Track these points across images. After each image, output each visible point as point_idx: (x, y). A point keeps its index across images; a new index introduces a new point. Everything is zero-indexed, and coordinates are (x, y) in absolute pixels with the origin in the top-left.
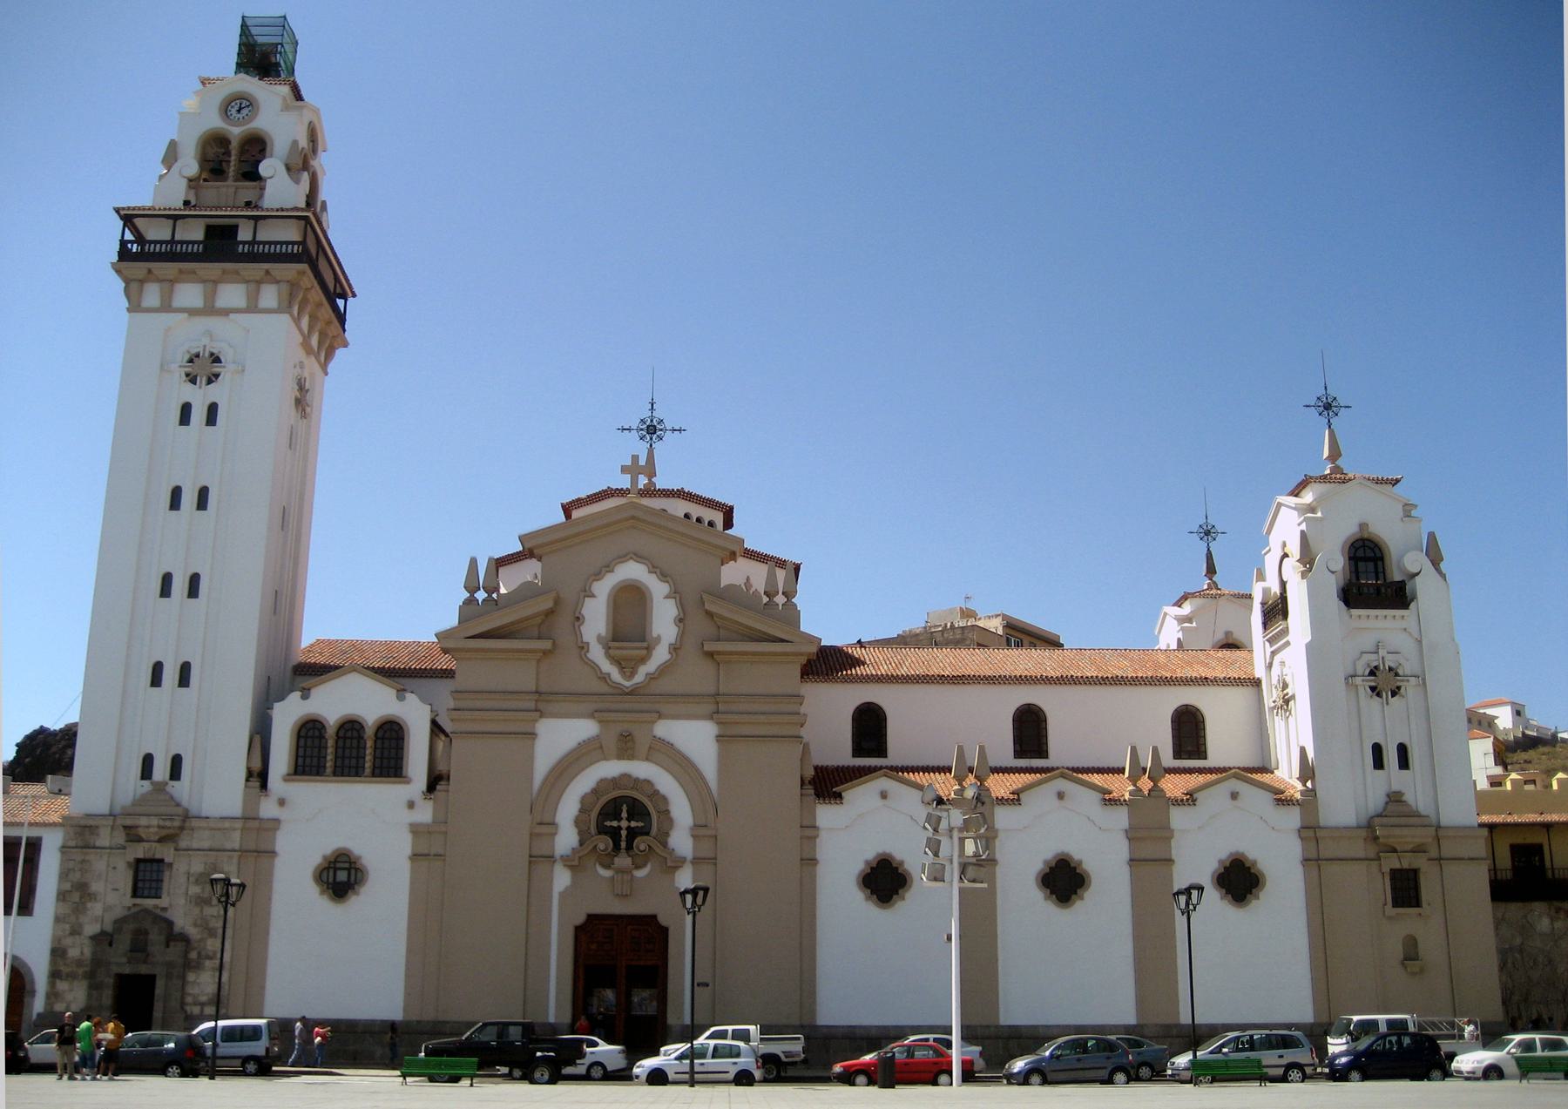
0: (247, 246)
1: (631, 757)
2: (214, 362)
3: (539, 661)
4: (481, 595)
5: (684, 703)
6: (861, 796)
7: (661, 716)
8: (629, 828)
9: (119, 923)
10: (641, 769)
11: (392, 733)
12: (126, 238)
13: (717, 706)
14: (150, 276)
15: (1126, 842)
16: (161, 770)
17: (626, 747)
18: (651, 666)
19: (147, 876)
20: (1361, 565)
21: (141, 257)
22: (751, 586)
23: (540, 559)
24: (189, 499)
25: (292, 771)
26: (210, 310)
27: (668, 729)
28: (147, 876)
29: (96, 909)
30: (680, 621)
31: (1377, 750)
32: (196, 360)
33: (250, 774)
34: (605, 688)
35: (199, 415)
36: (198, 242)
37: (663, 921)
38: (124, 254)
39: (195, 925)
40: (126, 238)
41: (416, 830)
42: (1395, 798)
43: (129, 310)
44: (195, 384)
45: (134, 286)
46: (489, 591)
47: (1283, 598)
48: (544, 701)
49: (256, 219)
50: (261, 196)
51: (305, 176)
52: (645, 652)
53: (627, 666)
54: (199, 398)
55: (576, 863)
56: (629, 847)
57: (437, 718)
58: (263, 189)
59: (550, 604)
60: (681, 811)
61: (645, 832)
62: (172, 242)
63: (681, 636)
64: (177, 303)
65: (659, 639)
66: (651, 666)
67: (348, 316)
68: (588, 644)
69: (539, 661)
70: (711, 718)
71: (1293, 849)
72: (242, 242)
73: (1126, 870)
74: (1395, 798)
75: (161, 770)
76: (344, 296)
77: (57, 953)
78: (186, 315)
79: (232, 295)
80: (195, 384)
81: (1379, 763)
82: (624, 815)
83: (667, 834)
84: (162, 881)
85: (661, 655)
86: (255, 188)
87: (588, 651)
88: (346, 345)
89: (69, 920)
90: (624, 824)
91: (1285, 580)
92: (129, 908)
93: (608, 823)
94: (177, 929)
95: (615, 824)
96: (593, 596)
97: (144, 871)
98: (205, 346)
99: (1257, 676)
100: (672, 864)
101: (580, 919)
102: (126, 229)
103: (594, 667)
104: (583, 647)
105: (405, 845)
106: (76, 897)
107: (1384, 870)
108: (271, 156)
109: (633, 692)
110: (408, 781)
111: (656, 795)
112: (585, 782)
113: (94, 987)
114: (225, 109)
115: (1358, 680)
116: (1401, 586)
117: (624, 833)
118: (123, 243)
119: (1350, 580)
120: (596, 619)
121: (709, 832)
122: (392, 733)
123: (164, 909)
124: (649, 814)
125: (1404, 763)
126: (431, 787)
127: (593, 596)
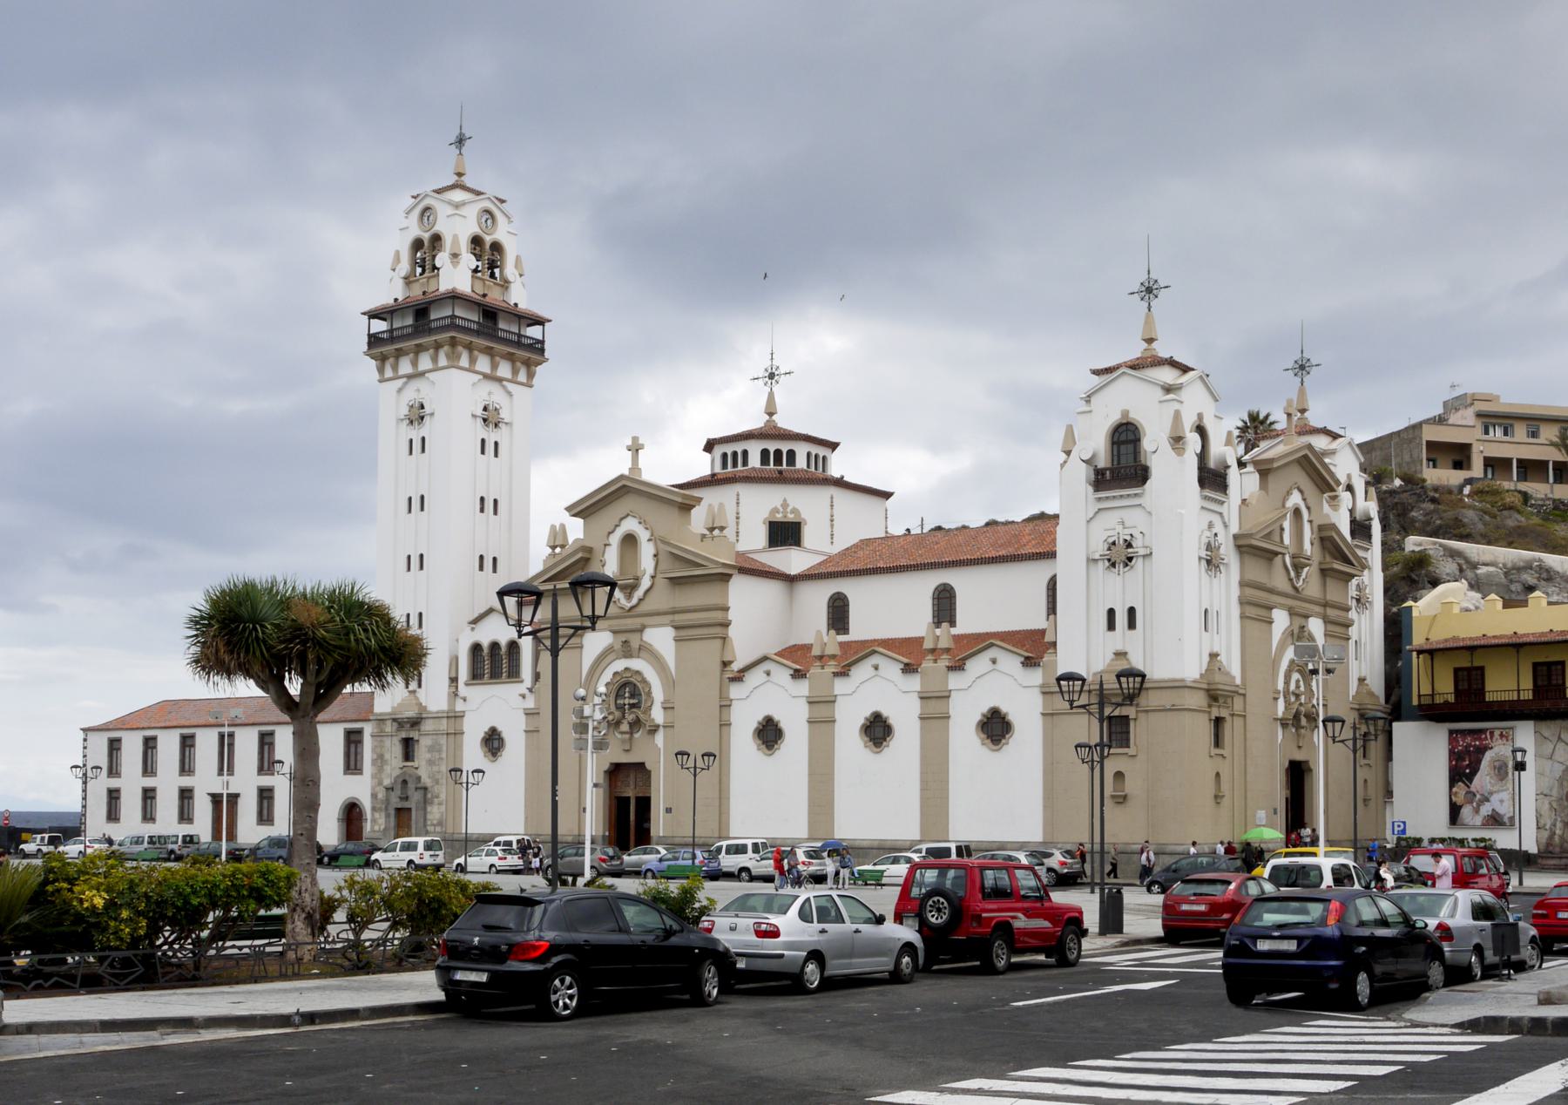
8: (629, 704)
10: (636, 664)
17: (627, 651)
28: (408, 747)
29: (388, 769)
37: (648, 766)
38: (374, 340)
39: (429, 777)
54: (415, 434)
60: (658, 694)
66: (639, 593)
77: (374, 796)
78: (405, 380)
79: (425, 362)
82: (627, 695)
85: (645, 583)
89: (377, 776)
92: (401, 768)
94: (422, 780)
101: (606, 767)
106: (379, 761)
110: (522, 682)
111: (644, 681)
112: (607, 676)
113: (388, 816)
118: (370, 336)
123: (417, 768)
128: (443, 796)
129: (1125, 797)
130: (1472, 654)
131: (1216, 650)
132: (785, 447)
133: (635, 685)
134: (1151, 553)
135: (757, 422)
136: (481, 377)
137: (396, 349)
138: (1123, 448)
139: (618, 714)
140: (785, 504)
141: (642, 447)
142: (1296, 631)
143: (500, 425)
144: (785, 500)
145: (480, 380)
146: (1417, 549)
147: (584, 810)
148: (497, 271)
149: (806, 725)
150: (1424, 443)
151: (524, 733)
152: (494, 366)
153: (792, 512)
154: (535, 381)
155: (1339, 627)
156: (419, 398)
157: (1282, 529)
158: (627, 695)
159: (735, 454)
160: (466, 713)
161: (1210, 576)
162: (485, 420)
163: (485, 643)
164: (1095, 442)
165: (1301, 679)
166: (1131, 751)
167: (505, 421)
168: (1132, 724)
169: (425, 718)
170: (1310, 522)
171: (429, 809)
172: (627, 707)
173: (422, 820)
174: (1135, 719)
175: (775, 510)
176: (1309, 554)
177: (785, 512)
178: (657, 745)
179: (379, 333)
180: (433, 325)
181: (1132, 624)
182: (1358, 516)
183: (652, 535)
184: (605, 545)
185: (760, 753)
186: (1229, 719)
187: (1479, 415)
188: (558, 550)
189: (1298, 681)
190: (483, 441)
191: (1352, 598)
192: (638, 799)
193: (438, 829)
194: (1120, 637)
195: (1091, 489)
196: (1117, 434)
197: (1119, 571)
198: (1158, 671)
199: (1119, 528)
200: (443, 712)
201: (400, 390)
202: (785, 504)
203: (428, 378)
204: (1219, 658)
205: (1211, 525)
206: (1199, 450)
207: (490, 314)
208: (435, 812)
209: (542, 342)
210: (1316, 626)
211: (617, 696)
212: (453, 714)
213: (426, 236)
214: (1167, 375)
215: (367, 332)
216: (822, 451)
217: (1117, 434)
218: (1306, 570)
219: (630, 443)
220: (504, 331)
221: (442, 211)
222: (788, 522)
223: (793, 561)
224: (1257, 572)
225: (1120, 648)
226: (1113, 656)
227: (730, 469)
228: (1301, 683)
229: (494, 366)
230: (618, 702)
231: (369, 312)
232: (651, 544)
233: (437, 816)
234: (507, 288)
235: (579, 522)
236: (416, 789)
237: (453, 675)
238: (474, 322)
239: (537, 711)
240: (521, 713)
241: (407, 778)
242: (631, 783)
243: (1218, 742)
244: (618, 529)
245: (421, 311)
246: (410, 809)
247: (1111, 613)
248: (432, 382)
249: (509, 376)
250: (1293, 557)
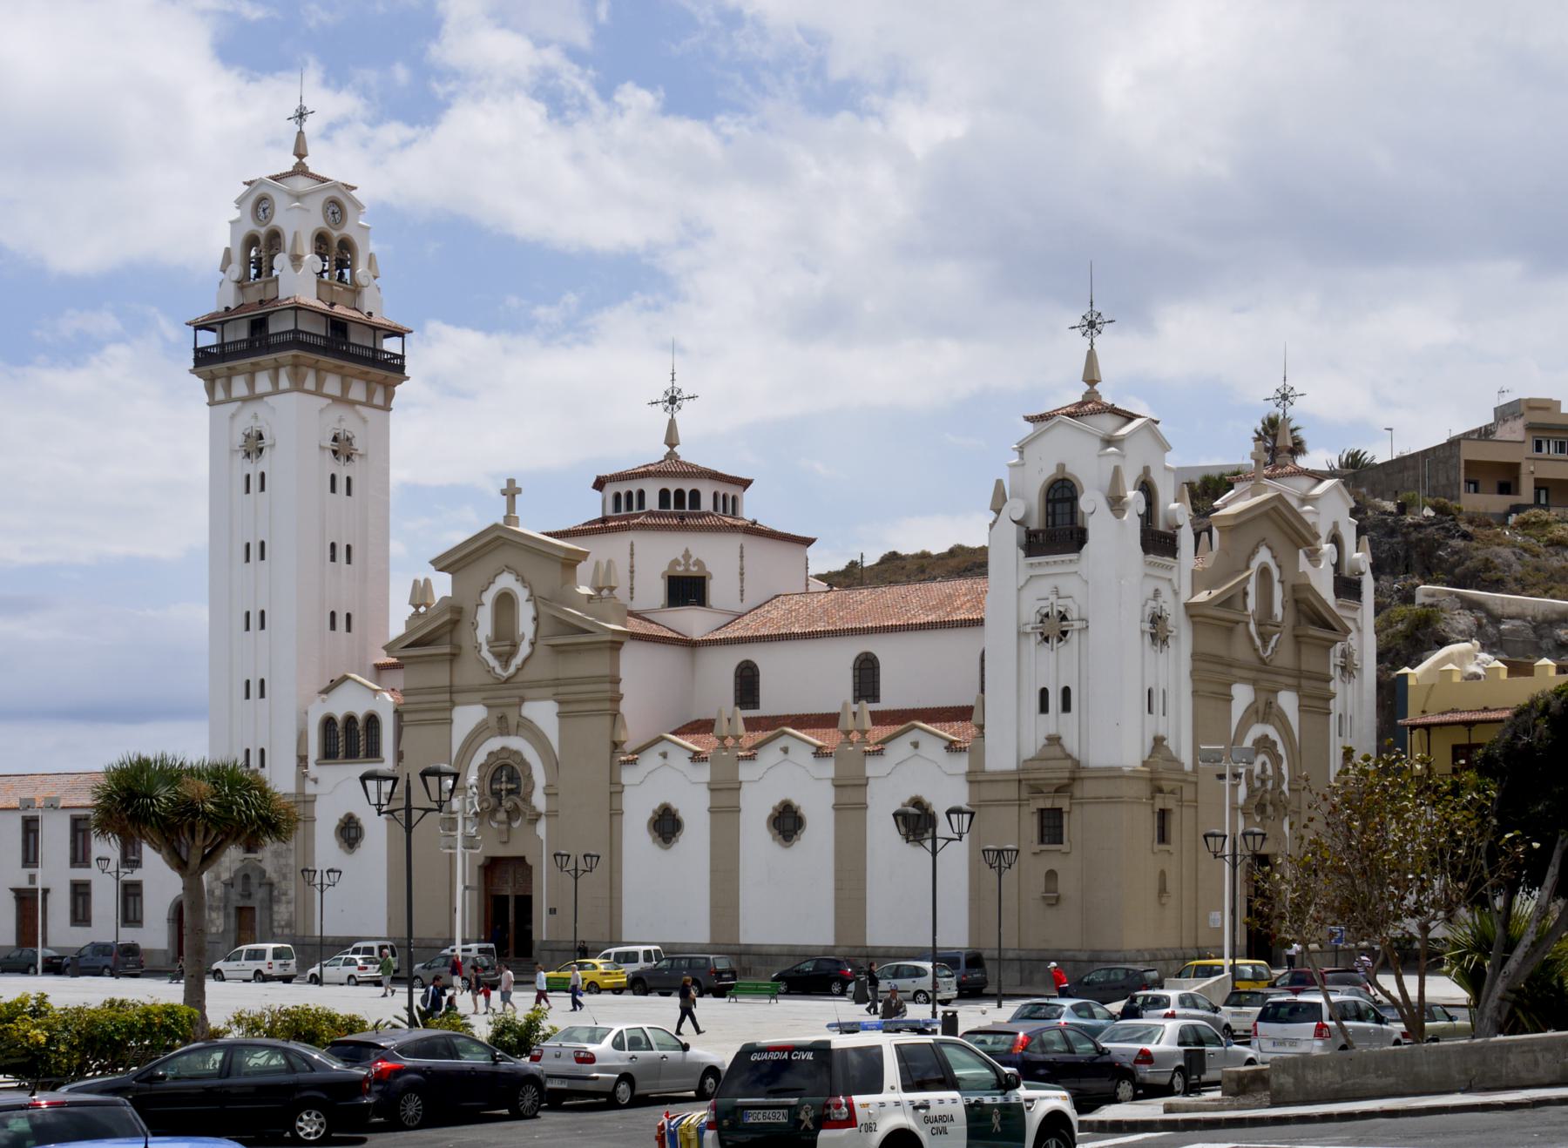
1: (508, 734)
3: (451, 661)
5: (538, 688)
7: (523, 700)
8: (507, 790)
9: (237, 872)
10: (515, 743)
11: (372, 721)
13: (556, 688)
17: (503, 727)
26: (253, 397)
37: (529, 861)
38: (203, 358)
39: (275, 871)
43: (210, 404)
46: (427, 606)
48: (454, 695)
53: (505, 658)
54: (253, 468)
60: (539, 776)
66: (517, 661)
68: (480, 644)
69: (451, 661)
78: (239, 403)
79: (263, 383)
82: (504, 779)
83: (530, 794)
85: (524, 649)
92: (243, 861)
94: (267, 875)
95: (498, 787)
96: (483, 604)
101: (481, 861)
104: (478, 648)
109: (508, 680)
111: (524, 763)
112: (480, 757)
113: (227, 916)
115: (1077, 625)
118: (197, 350)
123: (260, 861)
127: (483, 604)
128: (292, 893)
129: (1058, 899)
130: (1469, 730)
131: (1161, 733)
132: (687, 486)
133: (513, 767)
134: (1087, 627)
135: (655, 452)
136: (330, 401)
137: (229, 368)
138: (1058, 506)
139: (493, 801)
140: (687, 555)
141: (519, 491)
142: (1261, 707)
143: (353, 457)
144: (687, 551)
145: (328, 405)
146: (1428, 601)
148: (347, 272)
149: (708, 815)
150: (1462, 465)
152: (345, 388)
153: (694, 565)
154: (394, 404)
155: (1317, 703)
157: (1246, 594)
158: (504, 779)
159: (629, 494)
161: (1156, 651)
162: (335, 452)
163: (339, 716)
164: (1028, 502)
165: (1268, 761)
166: (1064, 847)
167: (360, 452)
168: (1065, 817)
170: (1282, 582)
171: (276, 908)
172: (503, 793)
173: (268, 921)
174: (1069, 812)
175: (675, 562)
176: (1279, 619)
177: (687, 564)
179: (207, 347)
180: (273, 340)
181: (1066, 707)
182: (1346, 573)
183: (531, 595)
184: (477, 606)
186: (1176, 810)
187: (1530, 428)
188: (422, 609)
189: (1264, 764)
190: (333, 477)
191: (1335, 665)
192: (517, 898)
193: (287, 931)
194: (1054, 721)
195: (1022, 553)
196: (1052, 491)
197: (1052, 646)
198: (1098, 755)
199: (1053, 598)
200: (291, 795)
201: (233, 417)
202: (687, 555)
203: (266, 402)
204: (1165, 743)
205: (1157, 593)
206: (1142, 509)
207: (339, 326)
208: (282, 912)
209: (402, 357)
210: (1288, 701)
211: (493, 780)
212: (302, 799)
213: (263, 231)
214: (1107, 423)
215: (193, 346)
216: (731, 491)
217: (1052, 491)
218: (1275, 638)
219: (505, 486)
220: (356, 345)
221: (281, 203)
222: (691, 577)
223: (692, 622)
224: (1215, 645)
225: (1052, 731)
226: (1045, 742)
227: (623, 512)
228: (1269, 766)
229: (345, 388)
230: (494, 787)
232: (531, 604)
233: (286, 917)
234: (359, 293)
235: (446, 578)
236: (260, 885)
238: (321, 337)
241: (249, 872)
242: (510, 880)
243: (1163, 837)
244: (492, 586)
246: (253, 909)
247: (1044, 693)
249: (363, 398)
250: (1259, 624)
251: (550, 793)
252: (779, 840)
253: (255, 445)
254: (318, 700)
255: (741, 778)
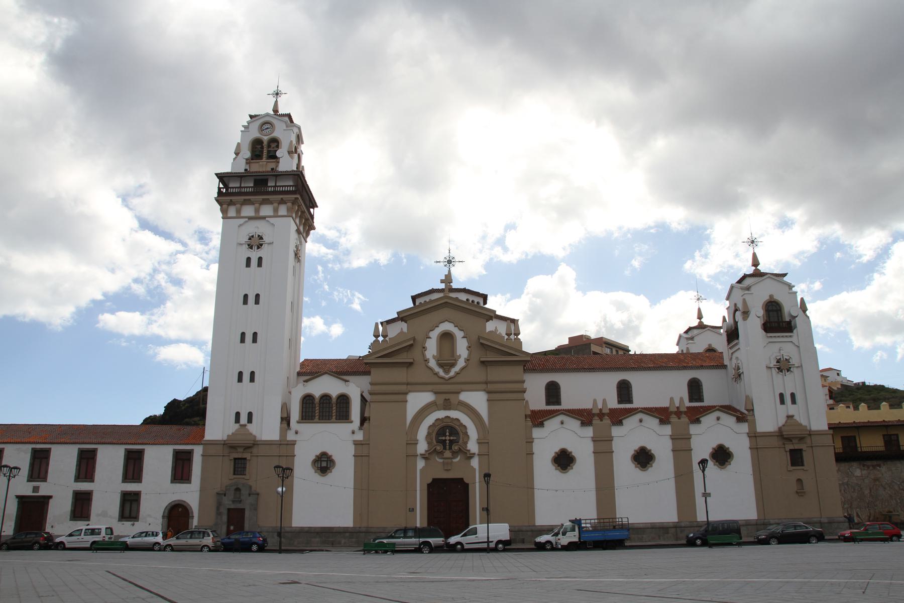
0: (272, 188)
1: (450, 409)
2: (260, 239)
4: (381, 339)
5: (472, 385)
6: (552, 424)
8: (450, 440)
10: (454, 414)
11: (344, 399)
12: (220, 186)
13: (486, 386)
14: (231, 203)
15: (671, 441)
16: (244, 419)
17: (447, 406)
18: (457, 369)
19: (240, 465)
20: (771, 313)
21: (227, 194)
22: (497, 330)
23: (406, 322)
24: (251, 299)
25: (301, 418)
26: (257, 218)
27: (465, 397)
28: (240, 465)
30: (469, 348)
31: (782, 396)
32: (252, 238)
33: (282, 419)
34: (436, 380)
35: (254, 262)
36: (252, 187)
37: (466, 481)
38: (220, 193)
40: (220, 186)
41: (356, 443)
42: (790, 417)
43: (223, 218)
44: (252, 249)
45: (225, 206)
47: (736, 329)
49: (276, 176)
50: (277, 166)
51: (296, 156)
52: (454, 361)
54: (254, 255)
55: (427, 456)
56: (450, 448)
57: (363, 394)
58: (278, 162)
59: (412, 342)
61: (456, 442)
62: (240, 187)
63: (470, 355)
64: (242, 215)
65: (460, 356)
66: (457, 369)
67: (315, 216)
68: (429, 359)
70: (484, 390)
71: (745, 442)
72: (269, 186)
73: (671, 454)
74: (790, 417)
75: (244, 419)
76: (313, 208)
78: (247, 219)
79: (266, 210)
80: (252, 249)
81: (782, 402)
82: (447, 434)
83: (466, 443)
84: (246, 467)
85: (461, 363)
86: (274, 162)
87: (429, 362)
88: (314, 229)
90: (448, 438)
91: (737, 320)
93: (440, 438)
95: (444, 438)
96: (430, 338)
97: (241, 464)
98: (256, 232)
99: (725, 364)
100: (470, 456)
101: (430, 481)
102: (220, 183)
103: (430, 369)
104: (427, 361)
105: (351, 449)
107: (787, 450)
108: (281, 148)
110: (352, 422)
112: (430, 420)
114: (261, 128)
116: (789, 323)
117: (448, 442)
118: (219, 188)
119: (766, 320)
120: (432, 348)
121: (487, 441)
122: (344, 399)
124: (458, 434)
125: (794, 401)
126: (362, 423)
127: (430, 338)
147: (412, 510)
149: (593, 455)
151: (354, 457)
156: (259, 232)
158: (447, 434)
160: (297, 442)
169: (258, 444)
178: (472, 467)
185: (558, 471)
188: (381, 339)
201: (240, 225)
212: (286, 443)
231: (219, 174)
237: (285, 415)
239: (368, 442)
240: (352, 442)
245: (261, 182)
248: (273, 224)
251: (480, 443)
252: (717, 465)
253: (256, 242)
254: (300, 386)
255: (613, 435)
